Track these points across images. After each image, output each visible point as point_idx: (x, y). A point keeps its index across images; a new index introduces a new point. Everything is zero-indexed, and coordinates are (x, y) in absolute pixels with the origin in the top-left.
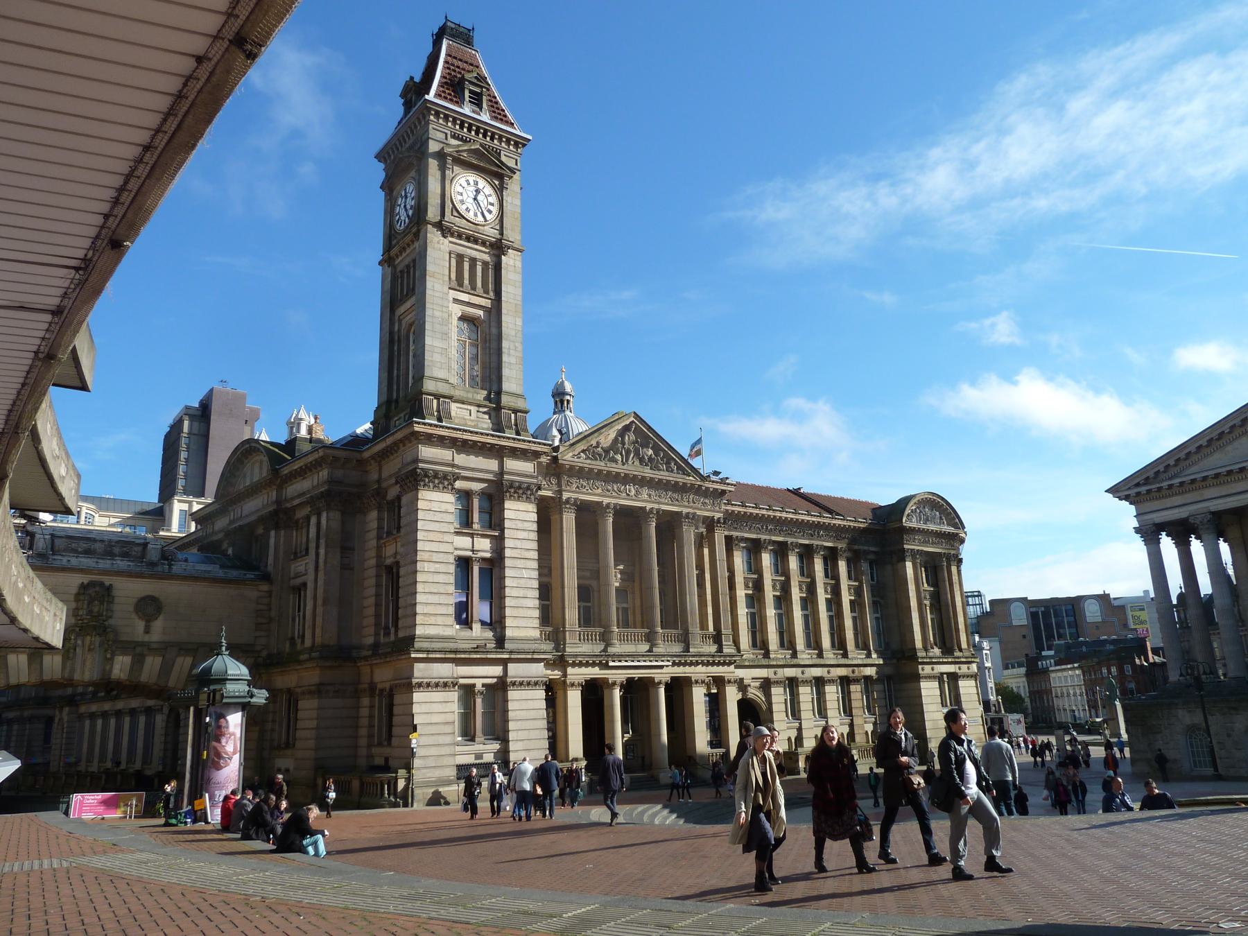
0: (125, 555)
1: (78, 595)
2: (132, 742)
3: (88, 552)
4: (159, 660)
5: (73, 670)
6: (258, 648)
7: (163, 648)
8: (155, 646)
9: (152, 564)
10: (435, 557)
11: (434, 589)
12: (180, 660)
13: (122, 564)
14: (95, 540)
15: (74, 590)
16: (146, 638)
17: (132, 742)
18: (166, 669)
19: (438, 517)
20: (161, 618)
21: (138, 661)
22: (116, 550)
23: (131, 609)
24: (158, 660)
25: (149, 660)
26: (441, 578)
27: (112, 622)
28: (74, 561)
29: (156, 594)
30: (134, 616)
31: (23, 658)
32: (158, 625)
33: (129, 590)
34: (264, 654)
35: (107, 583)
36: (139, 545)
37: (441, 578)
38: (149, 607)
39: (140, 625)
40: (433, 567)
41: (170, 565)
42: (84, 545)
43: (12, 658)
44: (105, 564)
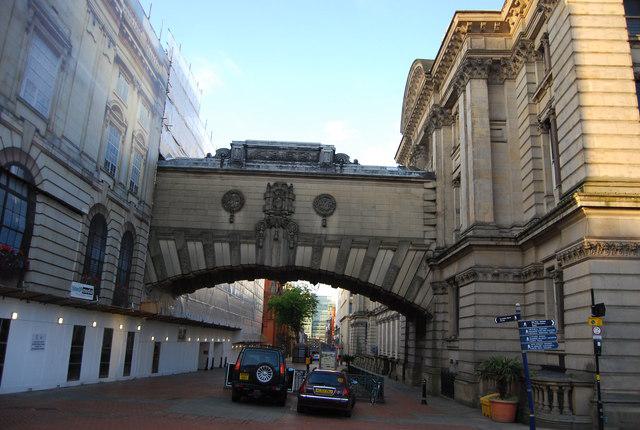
0: (304, 160)
1: (265, 194)
2: (394, 342)
3: (274, 159)
4: (336, 251)
5: (263, 257)
6: (427, 242)
7: (337, 242)
8: (330, 238)
9: (325, 165)
10: (602, 73)
11: (607, 114)
12: (354, 252)
13: (302, 168)
14: (278, 149)
15: (264, 190)
16: (324, 231)
17: (394, 337)
18: (343, 259)
19: (600, 22)
20: (336, 213)
21: (318, 251)
22: (296, 156)
23: (310, 205)
24: (336, 251)
25: (327, 251)
26: (615, 100)
27: (294, 217)
28: (263, 167)
29: (330, 193)
30: (313, 211)
31: (226, 246)
32: (333, 220)
33: (306, 191)
34: (433, 247)
35: (289, 184)
36: (314, 150)
37: (615, 100)
38: (325, 206)
39: (319, 220)
40: (602, 86)
41: (342, 167)
42: (270, 152)
43: (217, 246)
44: (288, 168)
